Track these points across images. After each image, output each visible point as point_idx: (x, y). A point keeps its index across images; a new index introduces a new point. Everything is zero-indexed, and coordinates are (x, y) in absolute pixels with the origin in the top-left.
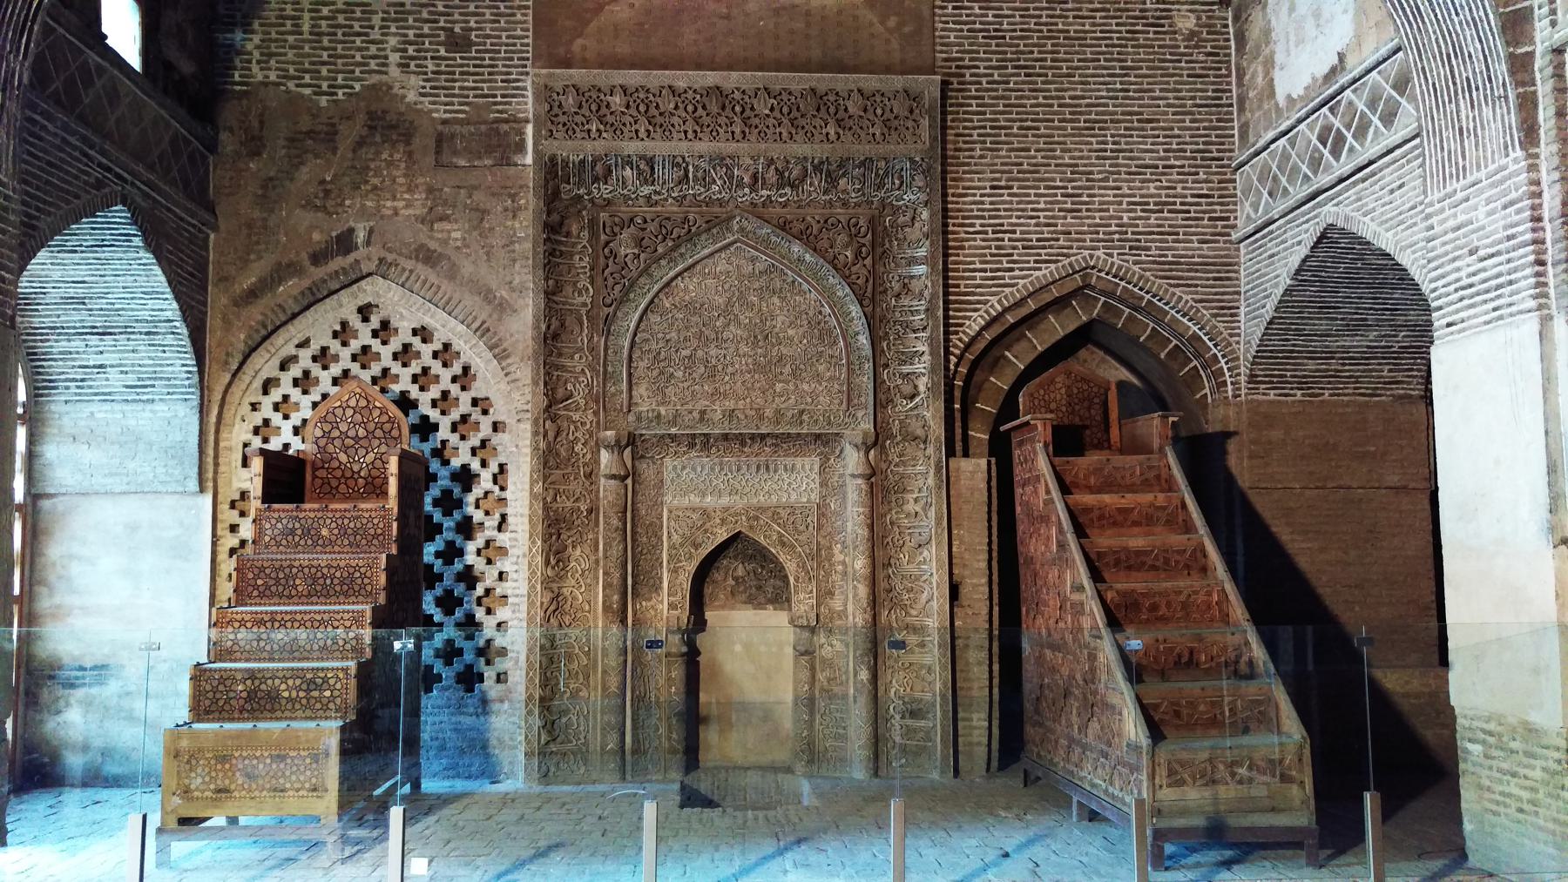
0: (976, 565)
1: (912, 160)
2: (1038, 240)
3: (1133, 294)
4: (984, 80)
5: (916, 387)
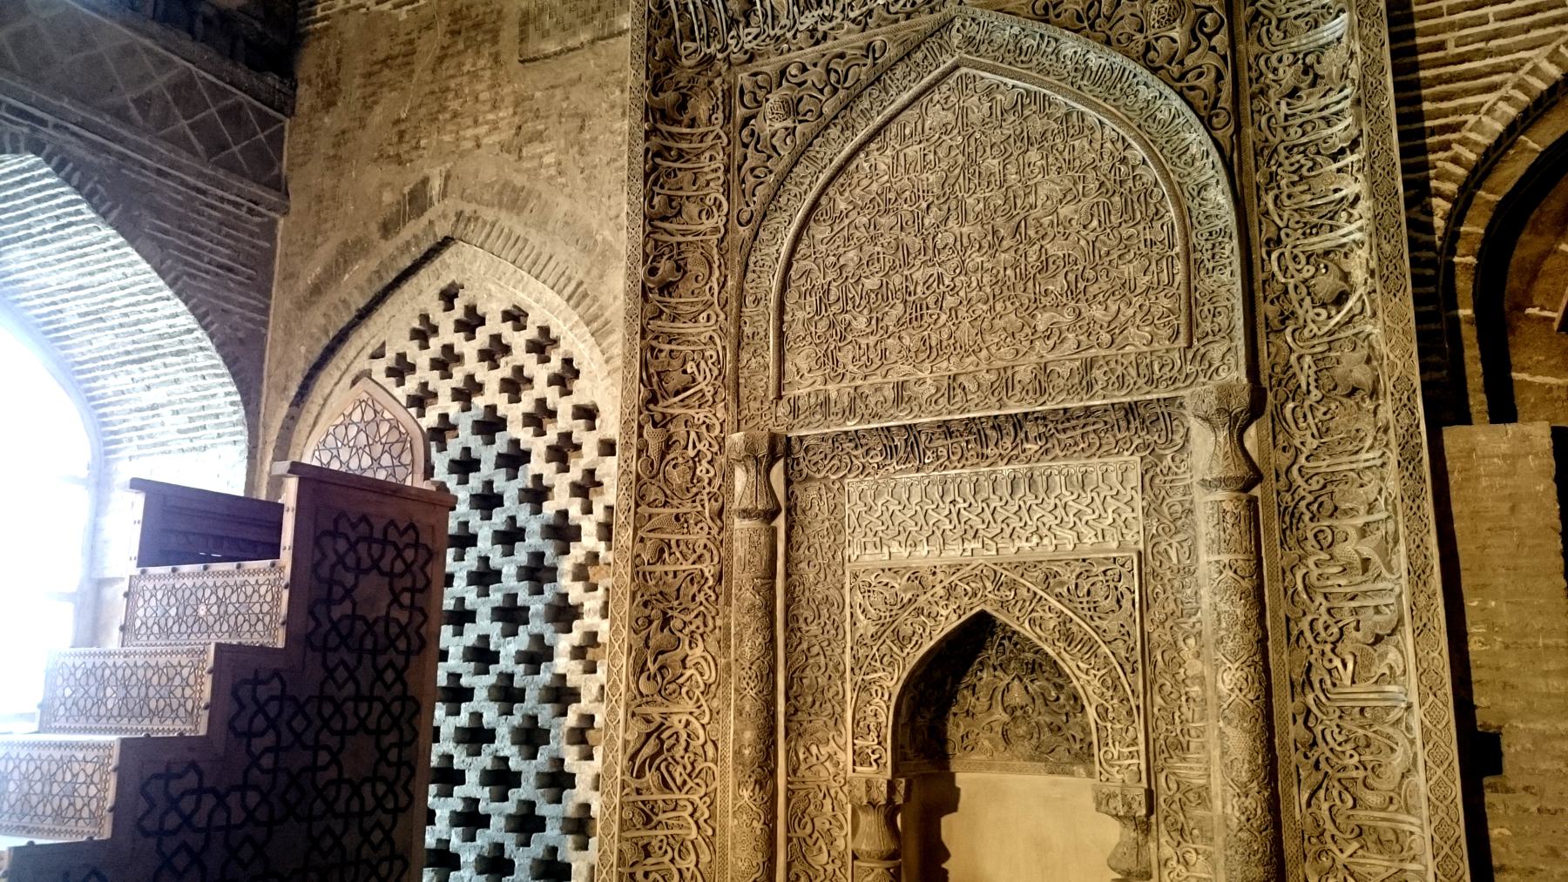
0: (1540, 685)
5: (1346, 276)
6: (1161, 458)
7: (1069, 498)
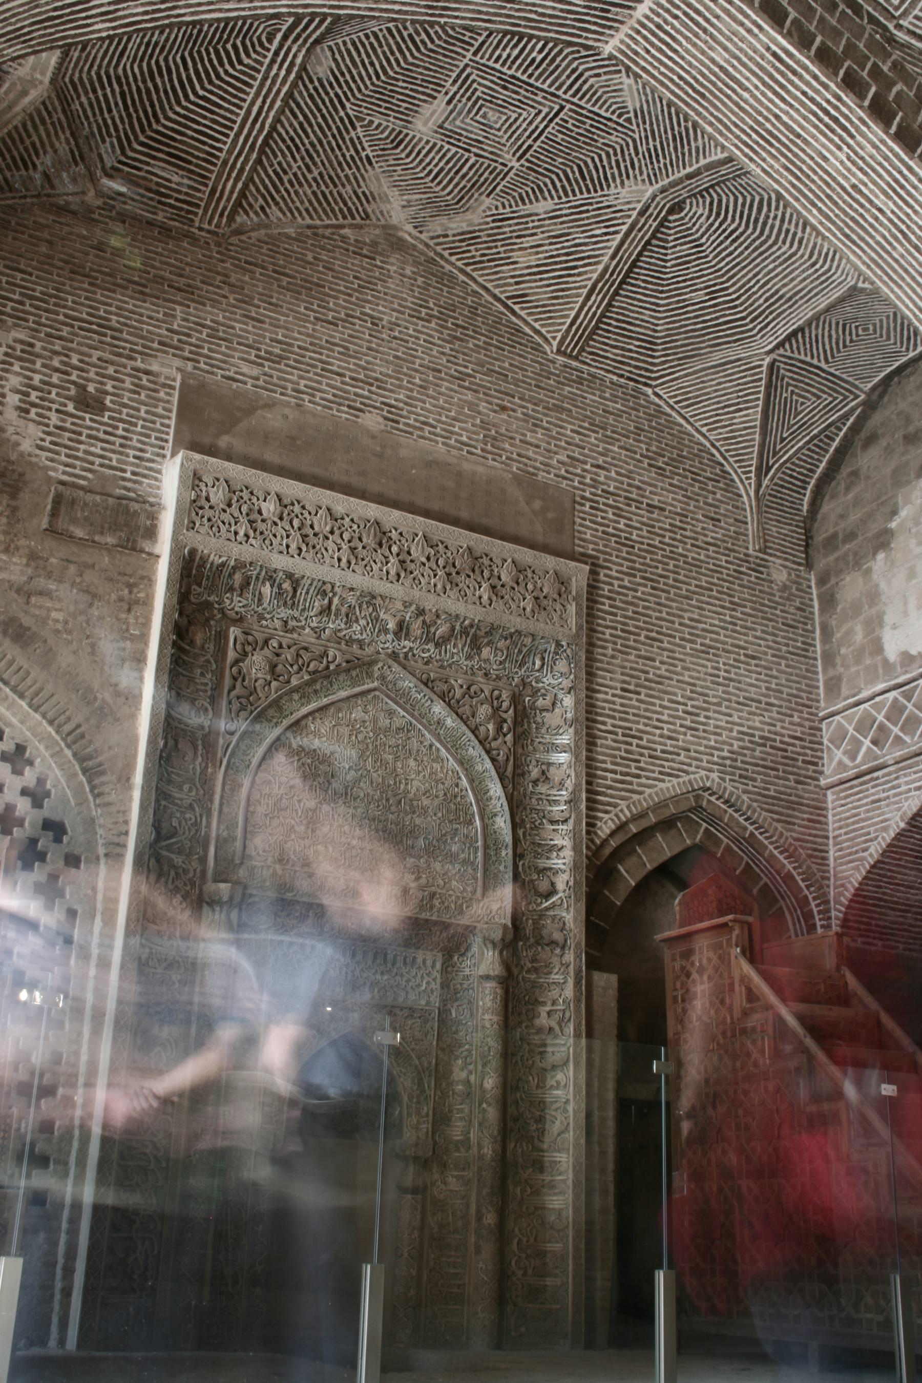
1: (558, 644)
3: (738, 823)
4: (616, 583)
5: (553, 884)
6: (451, 957)
7: (404, 971)
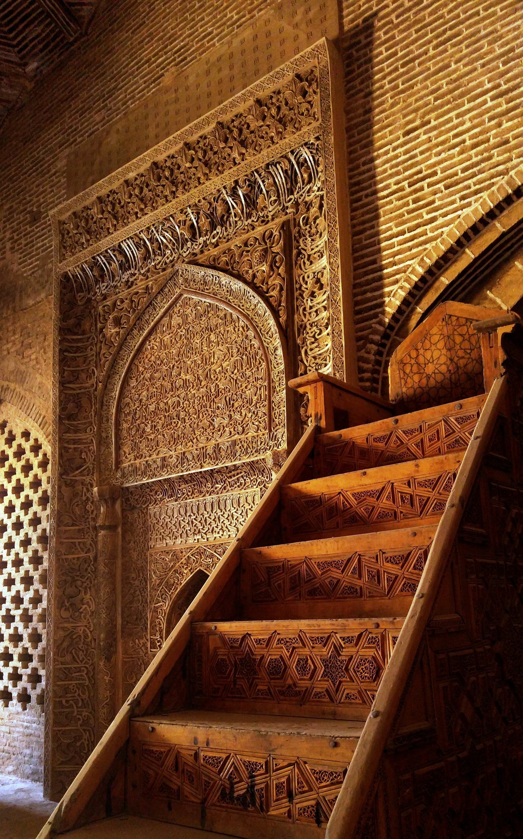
2: (464, 170)
